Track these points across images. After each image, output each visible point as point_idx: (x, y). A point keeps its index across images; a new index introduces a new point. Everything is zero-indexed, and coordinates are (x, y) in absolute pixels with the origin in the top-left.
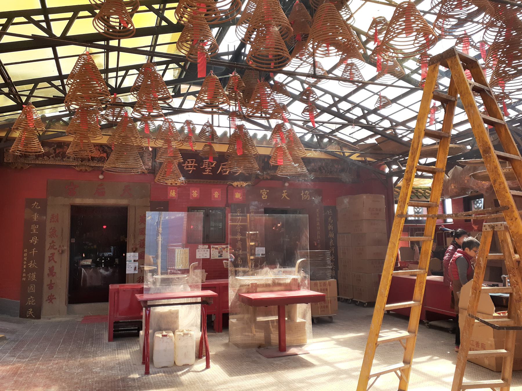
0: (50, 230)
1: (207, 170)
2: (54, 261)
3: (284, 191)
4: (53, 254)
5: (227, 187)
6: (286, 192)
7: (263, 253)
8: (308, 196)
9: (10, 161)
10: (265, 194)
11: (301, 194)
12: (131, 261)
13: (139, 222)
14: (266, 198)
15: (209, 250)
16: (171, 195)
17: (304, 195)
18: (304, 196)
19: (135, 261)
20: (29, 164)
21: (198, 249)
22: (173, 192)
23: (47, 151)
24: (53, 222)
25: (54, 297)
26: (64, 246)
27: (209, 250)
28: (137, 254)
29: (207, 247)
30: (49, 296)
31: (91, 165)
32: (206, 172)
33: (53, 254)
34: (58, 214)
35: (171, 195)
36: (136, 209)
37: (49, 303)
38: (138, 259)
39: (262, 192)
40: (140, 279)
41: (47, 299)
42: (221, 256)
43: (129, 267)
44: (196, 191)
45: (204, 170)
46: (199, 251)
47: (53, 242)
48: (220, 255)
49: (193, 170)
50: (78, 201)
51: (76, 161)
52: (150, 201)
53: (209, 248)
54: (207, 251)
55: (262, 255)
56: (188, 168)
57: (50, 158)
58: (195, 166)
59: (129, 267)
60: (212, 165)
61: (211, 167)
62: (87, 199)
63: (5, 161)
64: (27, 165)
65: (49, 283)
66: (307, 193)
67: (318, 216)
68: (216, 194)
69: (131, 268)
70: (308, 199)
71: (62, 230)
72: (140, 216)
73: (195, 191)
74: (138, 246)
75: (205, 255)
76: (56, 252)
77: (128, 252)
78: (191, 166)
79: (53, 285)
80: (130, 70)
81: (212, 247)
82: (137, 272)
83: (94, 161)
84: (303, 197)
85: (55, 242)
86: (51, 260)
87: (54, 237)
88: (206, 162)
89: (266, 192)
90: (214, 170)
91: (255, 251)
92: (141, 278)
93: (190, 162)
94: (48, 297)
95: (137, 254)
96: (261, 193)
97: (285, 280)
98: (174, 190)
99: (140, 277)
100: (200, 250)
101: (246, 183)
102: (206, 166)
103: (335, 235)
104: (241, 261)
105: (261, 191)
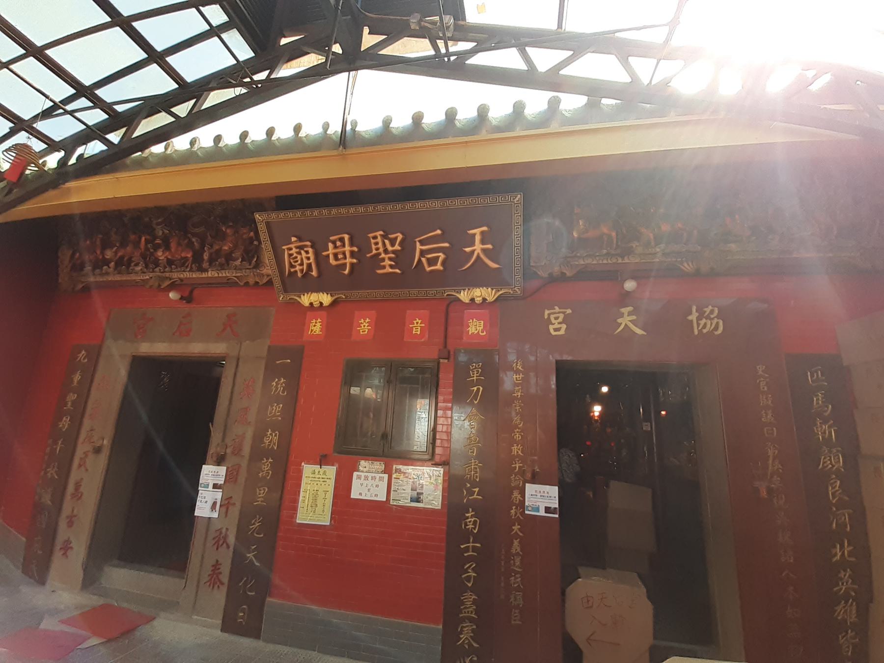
3: (623, 310)
5: (448, 305)
6: (630, 314)
8: (716, 320)
10: (560, 320)
14: (562, 332)
15: (386, 476)
16: (312, 330)
17: (699, 319)
19: (215, 486)
21: (358, 471)
22: (316, 323)
27: (386, 476)
28: (222, 470)
29: (379, 466)
32: (384, 267)
36: (240, 364)
38: (222, 482)
39: (549, 315)
40: (221, 533)
42: (418, 500)
43: (203, 500)
44: (368, 320)
46: (359, 477)
48: (415, 494)
49: (352, 265)
50: (146, 348)
53: (388, 471)
54: (381, 479)
55: (548, 510)
60: (393, 245)
61: (394, 252)
66: (712, 312)
68: (417, 326)
73: (365, 320)
75: (374, 490)
81: (396, 470)
82: (215, 515)
84: (698, 325)
89: (561, 316)
91: (523, 496)
95: (222, 470)
96: (546, 317)
98: (319, 320)
99: (221, 529)
100: (363, 474)
104: (475, 522)
105: (547, 312)
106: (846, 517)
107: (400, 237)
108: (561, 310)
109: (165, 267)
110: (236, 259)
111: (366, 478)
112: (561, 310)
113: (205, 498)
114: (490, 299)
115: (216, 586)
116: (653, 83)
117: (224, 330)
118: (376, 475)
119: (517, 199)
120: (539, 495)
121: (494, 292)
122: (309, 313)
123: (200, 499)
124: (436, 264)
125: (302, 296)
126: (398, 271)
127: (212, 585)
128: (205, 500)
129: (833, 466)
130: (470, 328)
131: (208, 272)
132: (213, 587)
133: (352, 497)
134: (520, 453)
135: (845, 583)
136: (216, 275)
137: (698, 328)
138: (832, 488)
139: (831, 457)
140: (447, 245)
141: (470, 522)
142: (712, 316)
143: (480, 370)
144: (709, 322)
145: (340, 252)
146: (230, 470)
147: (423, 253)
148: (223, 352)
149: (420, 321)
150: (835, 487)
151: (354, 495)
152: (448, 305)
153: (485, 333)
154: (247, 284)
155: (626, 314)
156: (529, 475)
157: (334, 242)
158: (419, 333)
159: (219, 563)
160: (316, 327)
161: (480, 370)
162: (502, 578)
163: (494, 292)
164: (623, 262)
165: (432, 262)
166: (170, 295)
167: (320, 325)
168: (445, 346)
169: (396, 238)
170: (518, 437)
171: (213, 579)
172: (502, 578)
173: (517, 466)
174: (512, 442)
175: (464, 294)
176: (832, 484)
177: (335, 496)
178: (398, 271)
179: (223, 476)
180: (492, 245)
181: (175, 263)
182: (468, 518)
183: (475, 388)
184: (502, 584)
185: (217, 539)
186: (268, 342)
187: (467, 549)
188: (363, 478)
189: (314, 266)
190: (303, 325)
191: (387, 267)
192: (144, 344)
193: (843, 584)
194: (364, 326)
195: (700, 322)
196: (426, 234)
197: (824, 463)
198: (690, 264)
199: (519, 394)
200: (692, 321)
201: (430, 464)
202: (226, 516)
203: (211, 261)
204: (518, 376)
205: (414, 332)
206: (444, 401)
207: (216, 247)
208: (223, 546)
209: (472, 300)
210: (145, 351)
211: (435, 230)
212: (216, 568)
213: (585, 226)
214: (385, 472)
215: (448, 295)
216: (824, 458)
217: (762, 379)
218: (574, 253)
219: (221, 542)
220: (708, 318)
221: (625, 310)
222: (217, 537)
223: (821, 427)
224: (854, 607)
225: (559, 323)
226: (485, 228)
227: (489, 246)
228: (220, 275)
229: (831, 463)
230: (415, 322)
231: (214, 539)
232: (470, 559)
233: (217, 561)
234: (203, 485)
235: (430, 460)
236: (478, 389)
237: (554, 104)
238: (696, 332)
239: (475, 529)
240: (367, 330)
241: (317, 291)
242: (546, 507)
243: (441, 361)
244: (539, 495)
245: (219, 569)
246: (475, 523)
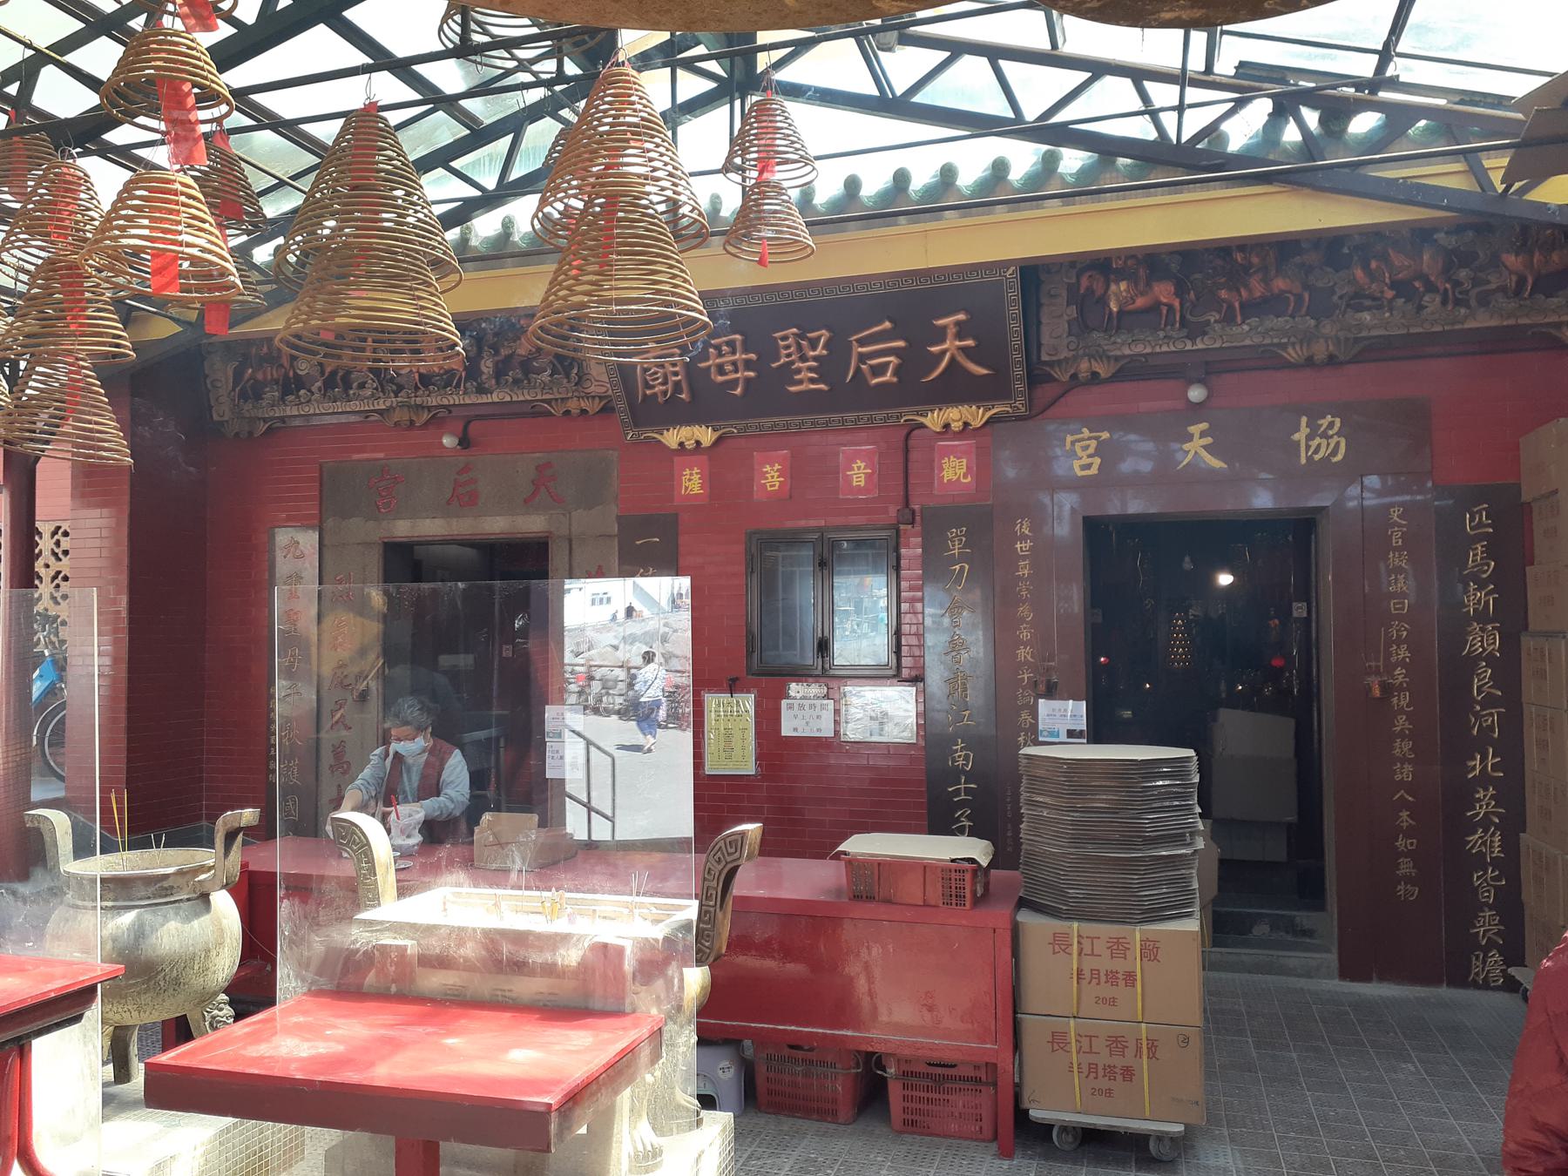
1: (799, 371)
3: (1192, 429)
5: (909, 434)
6: (1203, 434)
7: (1078, 728)
8: (1336, 439)
9: (226, 418)
10: (1091, 450)
11: (1296, 437)
16: (687, 488)
17: (1309, 438)
18: (1314, 443)
20: (265, 420)
21: (788, 697)
22: (691, 474)
23: (306, 371)
31: (429, 404)
32: (800, 382)
35: (687, 488)
36: (574, 546)
39: (1073, 443)
43: (556, 755)
44: (777, 467)
45: (787, 372)
46: (790, 707)
49: (748, 380)
50: (402, 529)
51: (381, 394)
56: (726, 374)
57: (313, 394)
58: (748, 365)
59: (556, 755)
60: (814, 348)
61: (815, 359)
63: (215, 417)
64: (262, 424)
66: (1331, 425)
67: (1397, 541)
70: (1335, 460)
78: (734, 363)
80: (985, 59)
83: (431, 387)
84: (1308, 447)
88: (785, 338)
90: (827, 369)
91: (1035, 714)
93: (724, 348)
97: (554, 949)
98: (696, 470)
101: (986, 411)
102: (789, 355)
103: (1511, 642)
105: (1069, 439)
106: (1492, 717)
107: (824, 335)
108: (1092, 435)
109: (417, 388)
110: (540, 371)
111: (801, 707)
112: (1092, 435)
113: (557, 752)
114: (977, 423)
116: (1184, 140)
117: (534, 494)
118: (815, 702)
119: (1010, 271)
120: (1058, 714)
121: (981, 411)
122: (676, 459)
124: (883, 373)
125: (665, 432)
126: (822, 386)
129: (1484, 650)
130: (945, 472)
131: (491, 394)
133: (783, 734)
134: (1029, 658)
135: (1484, 803)
136: (508, 399)
137: (1307, 453)
138: (1479, 681)
139: (1482, 637)
140: (901, 344)
141: (960, 756)
142: (1331, 433)
143: (964, 539)
144: (1324, 442)
145: (728, 362)
147: (863, 358)
149: (863, 465)
150: (1482, 680)
151: (786, 730)
152: (909, 434)
153: (969, 479)
154: (567, 413)
155: (1197, 436)
156: (1042, 687)
157: (718, 347)
158: (862, 484)
160: (692, 482)
161: (964, 539)
162: (1009, 825)
163: (981, 411)
164: (1195, 347)
165: (879, 370)
166: (445, 441)
167: (700, 479)
168: (907, 504)
169: (819, 338)
170: (1025, 635)
172: (1009, 825)
173: (1026, 676)
174: (1019, 643)
175: (933, 417)
176: (1478, 675)
177: (759, 734)
178: (822, 386)
180: (974, 338)
181: (433, 380)
182: (956, 751)
183: (958, 567)
184: (1009, 834)
186: (614, 510)
187: (957, 792)
188: (796, 706)
189: (684, 385)
190: (670, 481)
191: (806, 381)
193: (1481, 807)
194: (773, 477)
195: (1311, 443)
196: (868, 328)
197: (1471, 646)
198: (1298, 348)
199: (1026, 572)
200: (1298, 443)
201: (895, 681)
203: (499, 373)
204: (1023, 545)
205: (855, 484)
206: (911, 589)
207: (504, 352)
209: (947, 426)
211: (880, 322)
213: (1129, 292)
214: (827, 697)
215: (906, 421)
216: (1474, 639)
217: (1396, 529)
218: (1113, 339)
220: (1325, 436)
221: (1195, 429)
223: (1475, 595)
224: (1497, 838)
225: (1090, 456)
226: (961, 317)
227: (970, 342)
228: (515, 399)
229: (1482, 646)
230: (855, 466)
232: (962, 804)
235: (894, 676)
236: (962, 568)
237: (1050, 162)
238: (1303, 461)
239: (967, 765)
240: (777, 484)
241: (689, 422)
242: (1068, 730)
243: (902, 527)
244: (1058, 714)
246: (966, 758)
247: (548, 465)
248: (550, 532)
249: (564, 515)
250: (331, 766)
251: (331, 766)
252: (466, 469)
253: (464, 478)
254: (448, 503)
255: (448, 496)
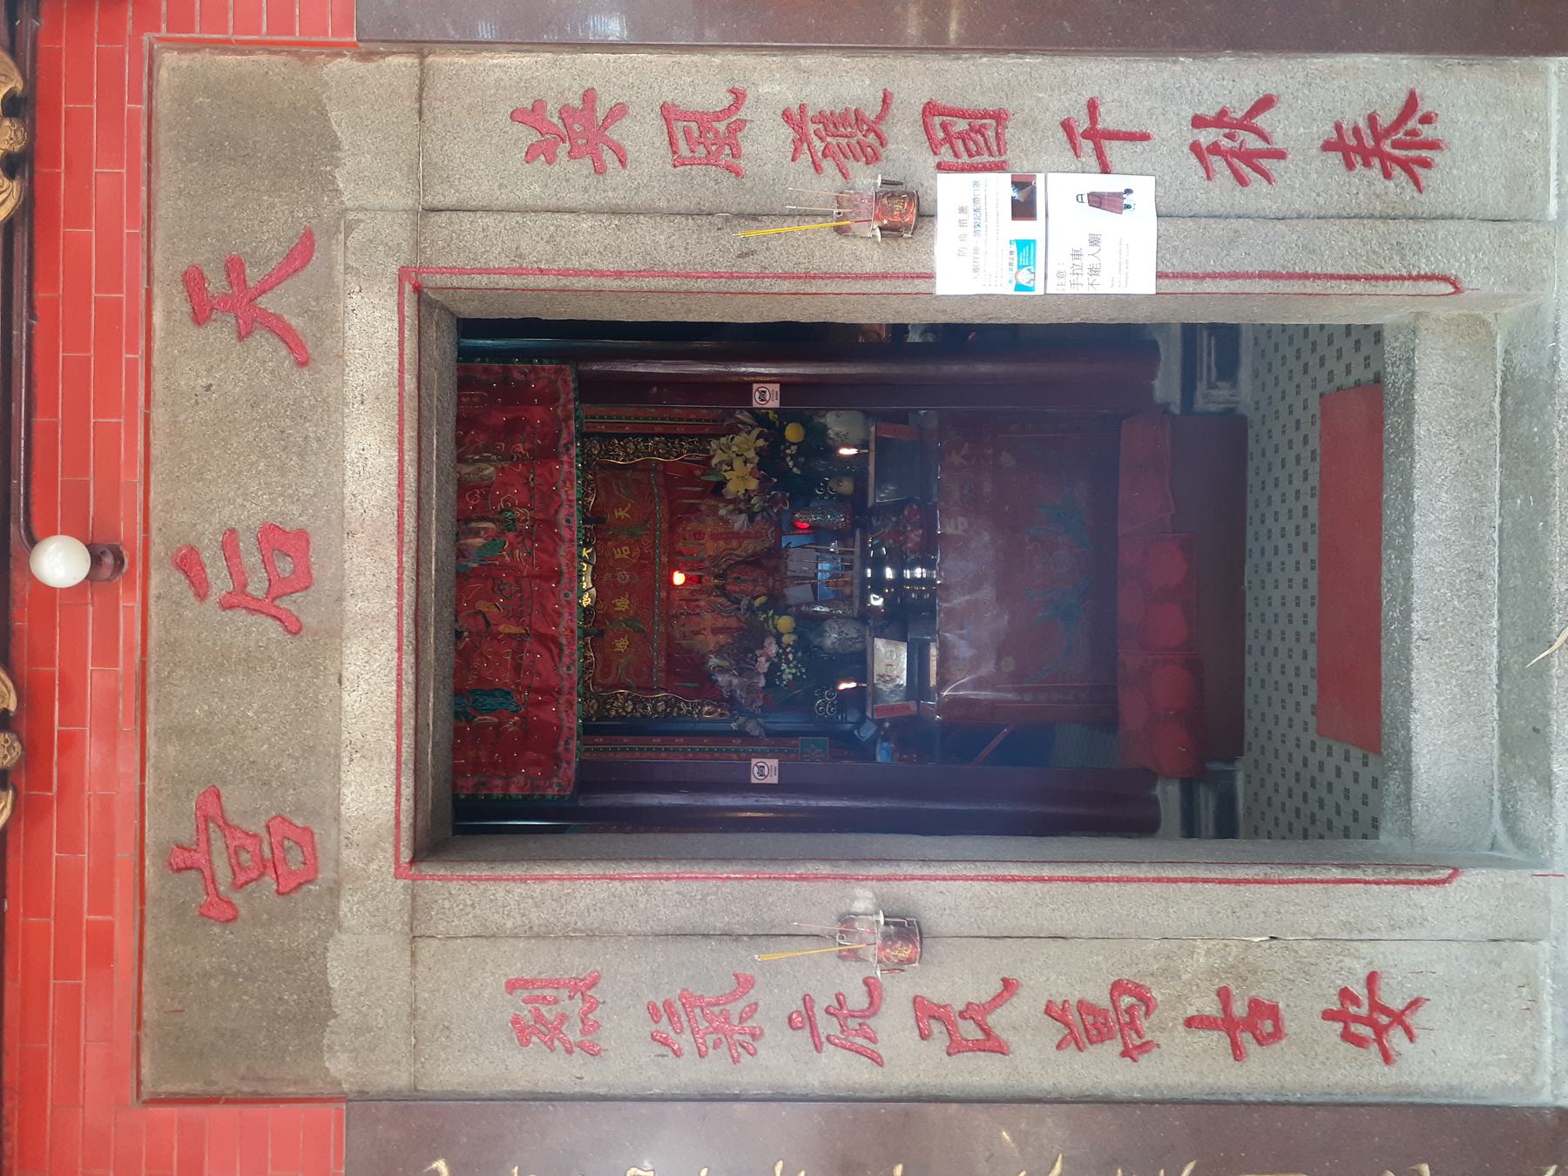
0: (677, 1053)
2: (997, 1001)
4: (927, 1013)
12: (1024, 246)
13: (600, 170)
19: (1023, 209)
24: (589, 1027)
25: (1360, 990)
26: (847, 920)
30: (1347, 1036)
33: (927, 1013)
34: (512, 986)
37: (1411, 1037)
38: (1005, 179)
40: (1215, 149)
41: (1374, 1047)
43: (1087, 261)
47: (802, 1020)
52: (367, 56)
59: (1087, 261)
62: (351, 700)
65: (1216, 1040)
69: (1094, 241)
71: (681, 935)
72: (530, 156)
74: (867, 180)
76: (899, 991)
77: (930, 276)
79: (1240, 1009)
82: (1143, 191)
85: (807, 1001)
86: (987, 1032)
87: (754, 1007)
92: (1207, 137)
94: (1359, 1041)
99: (1195, 148)
113: (1076, 255)
115: (1427, 132)
123: (1084, 279)
127: (1424, 153)
128: (1087, 249)
132: (1433, 145)
146: (946, 155)
148: (392, 303)
159: (1335, 135)
171: (1397, 152)
179: (975, 184)
185: (1236, 162)
192: (349, 795)
202: (1144, 137)
208: (1267, 129)
210: (389, 780)
212: (1352, 148)
219: (1253, 142)
222: (1230, 165)
231: (1242, 181)
233: (1327, 147)
234: (1024, 277)
245: (1356, 131)
247: (193, 281)
248: (403, 273)
249: (349, 229)
250: (1125, 1054)
251: (1125, 1054)
252: (188, 564)
253: (220, 581)
254: (293, 628)
255: (273, 629)
